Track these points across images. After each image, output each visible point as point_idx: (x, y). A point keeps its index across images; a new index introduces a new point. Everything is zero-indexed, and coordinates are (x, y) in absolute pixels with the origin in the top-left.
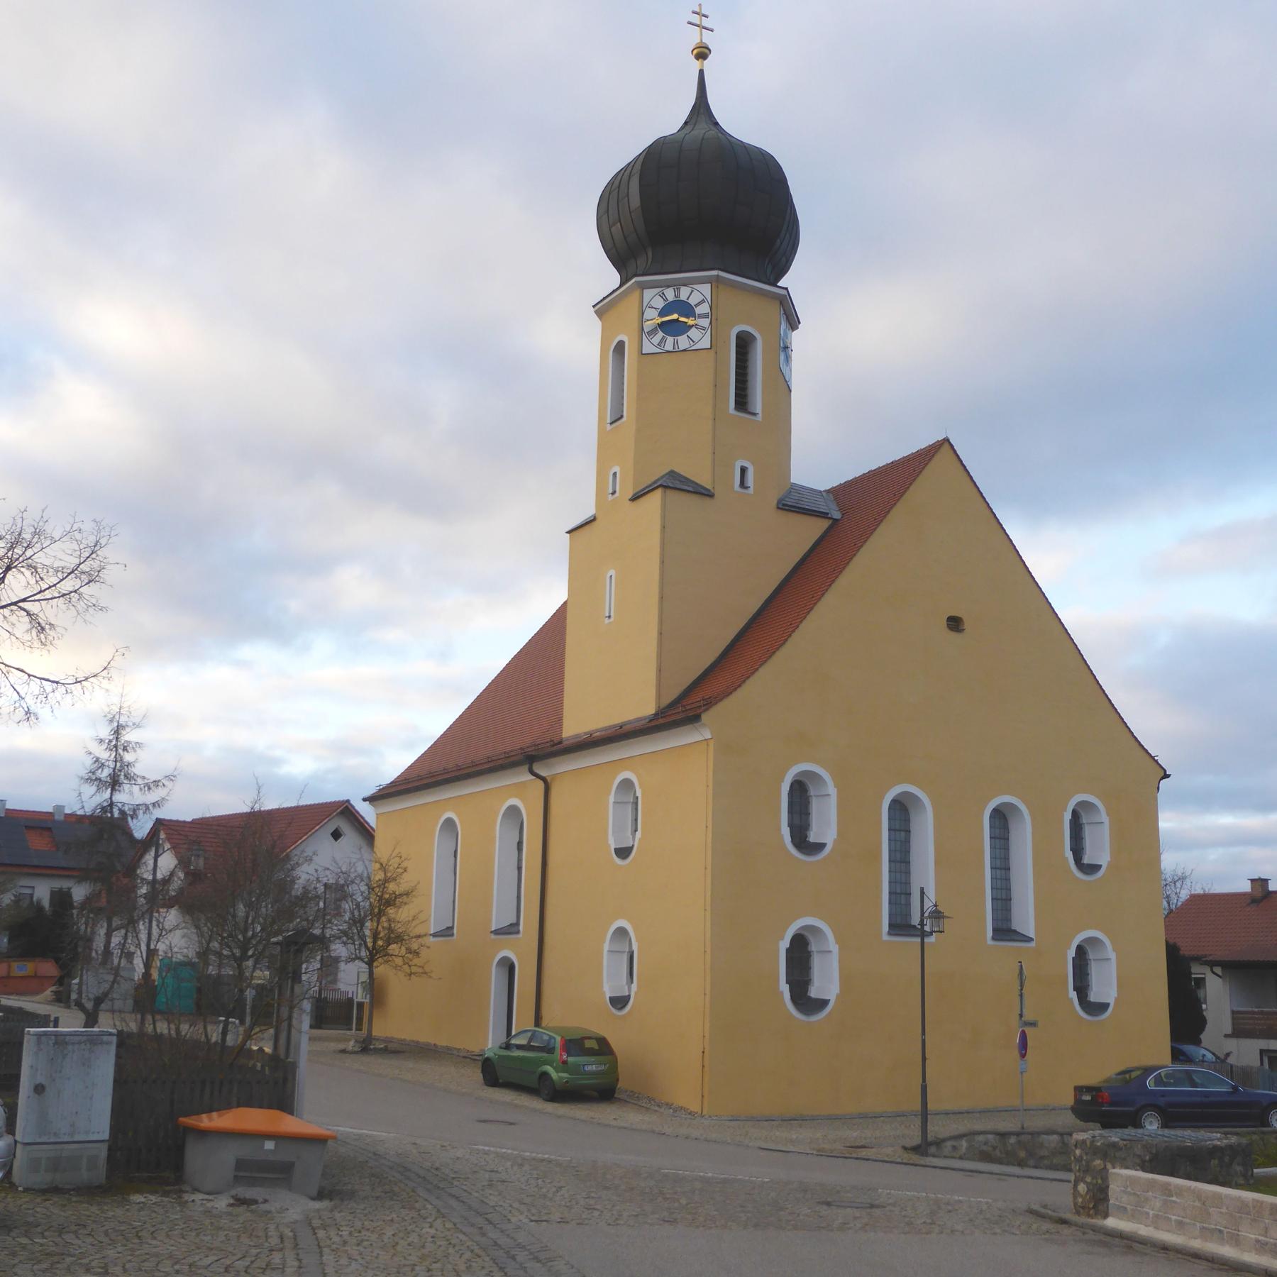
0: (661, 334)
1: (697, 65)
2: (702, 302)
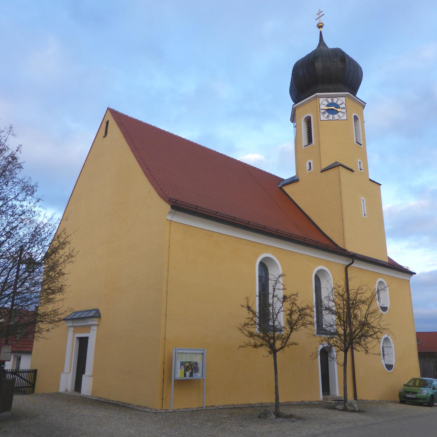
0: (327, 114)
1: (318, 30)
2: (342, 103)
